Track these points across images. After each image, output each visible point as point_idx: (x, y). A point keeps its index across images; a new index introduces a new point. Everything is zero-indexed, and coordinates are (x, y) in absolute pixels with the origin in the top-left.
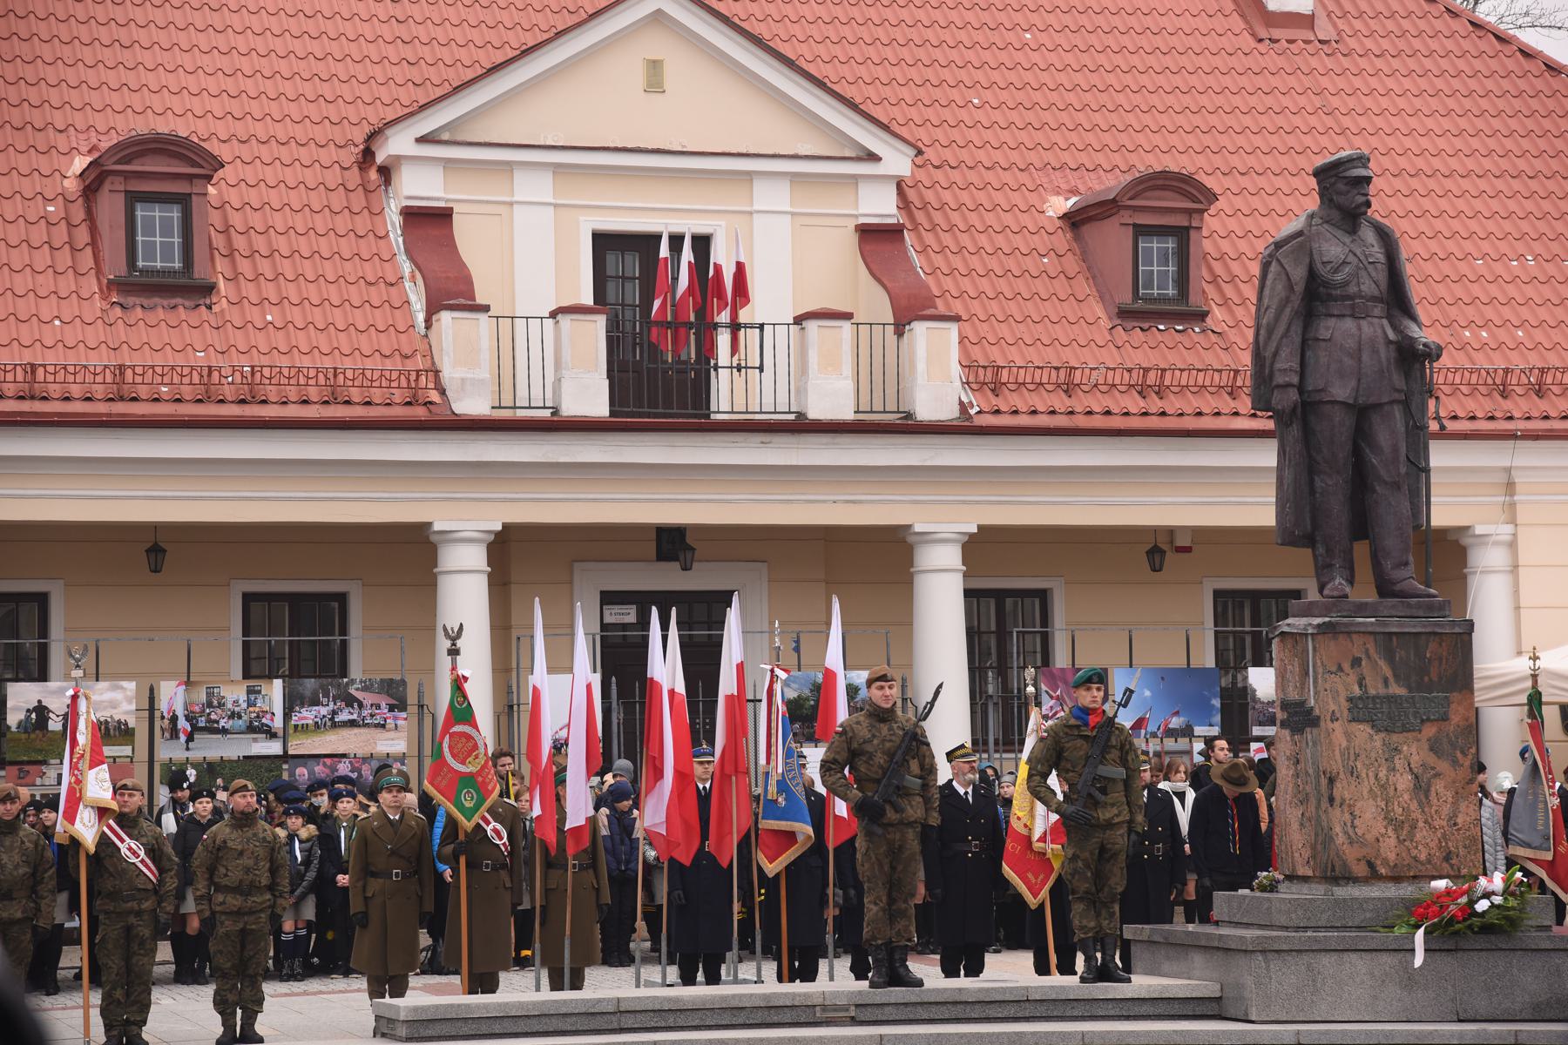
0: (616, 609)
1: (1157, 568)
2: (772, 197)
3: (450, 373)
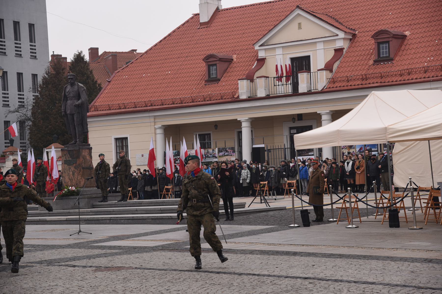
0: (293, 130)
2: (320, 46)
3: (240, 91)
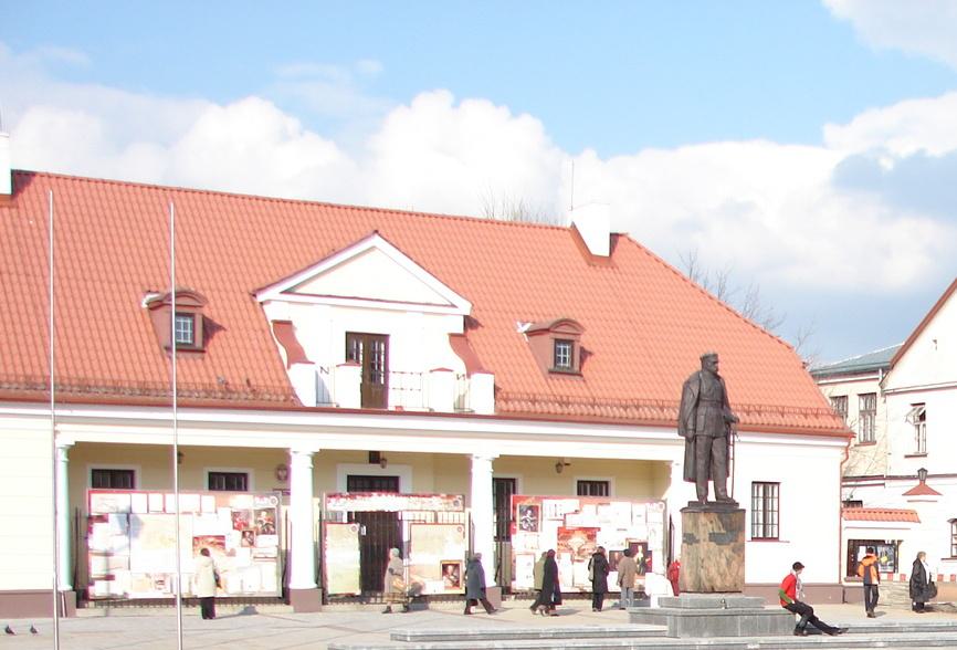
1: (559, 472)
